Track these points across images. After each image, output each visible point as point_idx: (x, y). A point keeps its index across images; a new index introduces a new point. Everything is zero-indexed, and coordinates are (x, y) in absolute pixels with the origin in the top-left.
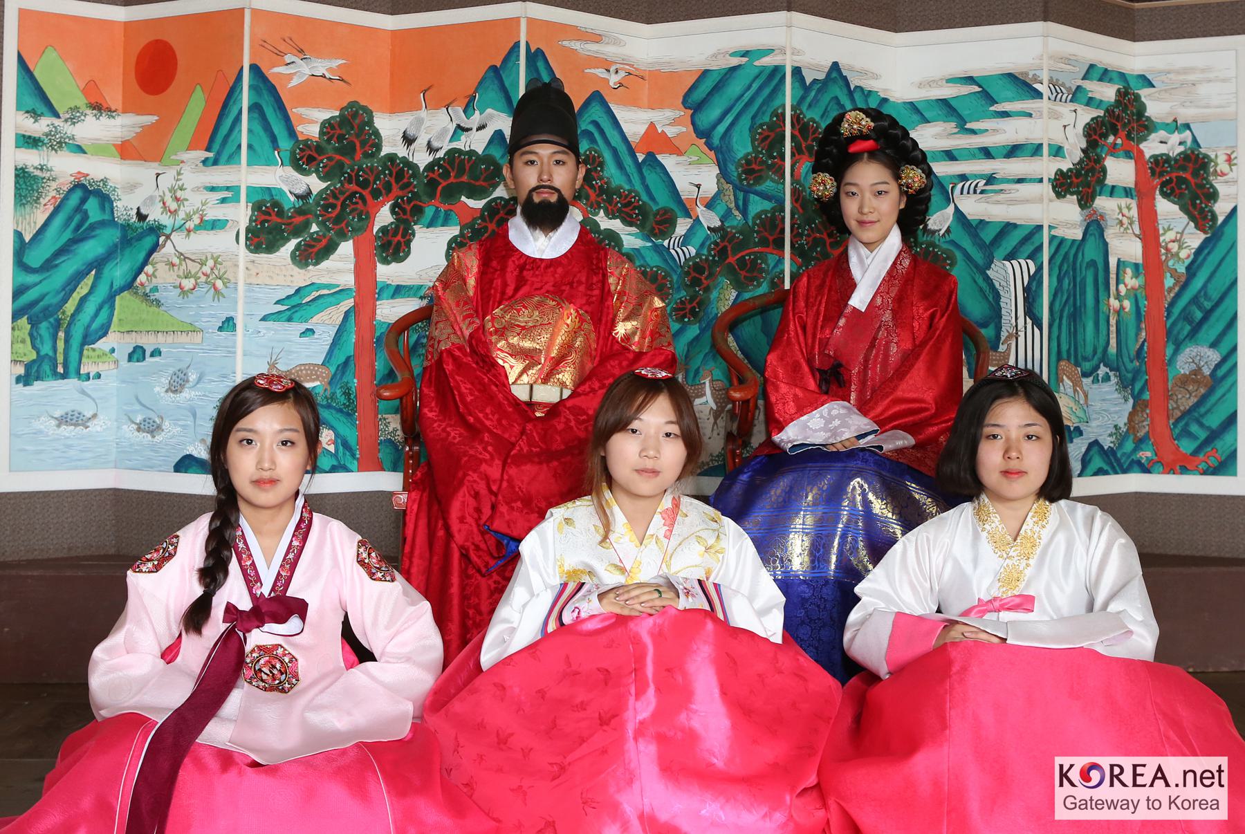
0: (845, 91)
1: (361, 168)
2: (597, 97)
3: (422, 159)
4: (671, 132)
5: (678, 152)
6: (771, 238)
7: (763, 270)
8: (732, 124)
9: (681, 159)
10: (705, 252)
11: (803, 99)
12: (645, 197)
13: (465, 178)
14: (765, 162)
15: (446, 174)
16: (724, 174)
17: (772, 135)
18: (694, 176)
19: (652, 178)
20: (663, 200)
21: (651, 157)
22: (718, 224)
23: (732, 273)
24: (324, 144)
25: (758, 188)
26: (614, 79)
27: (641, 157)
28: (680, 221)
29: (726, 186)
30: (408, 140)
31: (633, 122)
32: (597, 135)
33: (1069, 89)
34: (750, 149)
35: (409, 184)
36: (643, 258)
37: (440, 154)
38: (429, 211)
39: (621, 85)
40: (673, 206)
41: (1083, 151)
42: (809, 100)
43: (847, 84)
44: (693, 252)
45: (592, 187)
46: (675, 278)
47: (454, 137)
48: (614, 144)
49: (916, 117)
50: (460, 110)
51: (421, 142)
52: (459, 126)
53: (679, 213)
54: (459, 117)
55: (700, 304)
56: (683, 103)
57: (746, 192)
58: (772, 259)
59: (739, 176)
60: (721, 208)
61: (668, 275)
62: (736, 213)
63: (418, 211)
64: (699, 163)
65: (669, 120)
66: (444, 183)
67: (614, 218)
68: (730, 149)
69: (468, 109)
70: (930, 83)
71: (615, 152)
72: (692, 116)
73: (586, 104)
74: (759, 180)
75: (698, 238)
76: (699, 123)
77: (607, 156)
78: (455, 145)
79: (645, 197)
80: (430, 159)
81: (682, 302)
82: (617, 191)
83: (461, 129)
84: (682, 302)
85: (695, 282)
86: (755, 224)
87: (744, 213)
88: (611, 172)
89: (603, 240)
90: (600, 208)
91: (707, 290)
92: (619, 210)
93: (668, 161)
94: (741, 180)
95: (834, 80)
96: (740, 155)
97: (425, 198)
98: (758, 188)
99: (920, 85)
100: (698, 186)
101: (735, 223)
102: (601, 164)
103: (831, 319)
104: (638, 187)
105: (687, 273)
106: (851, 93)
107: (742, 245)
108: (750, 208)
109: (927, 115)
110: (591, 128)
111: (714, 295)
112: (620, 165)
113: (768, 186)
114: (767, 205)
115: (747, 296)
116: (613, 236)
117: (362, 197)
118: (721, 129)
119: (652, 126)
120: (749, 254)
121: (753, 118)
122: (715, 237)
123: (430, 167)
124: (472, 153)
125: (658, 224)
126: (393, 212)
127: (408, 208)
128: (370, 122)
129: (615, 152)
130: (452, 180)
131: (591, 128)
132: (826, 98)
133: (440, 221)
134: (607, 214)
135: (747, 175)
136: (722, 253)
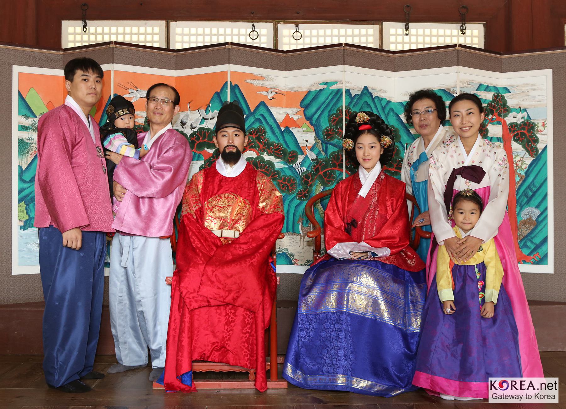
2: (262, 104)
3: (189, 132)
4: (295, 118)
5: (299, 127)
6: (337, 164)
7: (334, 178)
8: (321, 114)
9: (299, 129)
10: (310, 169)
11: (350, 103)
12: (285, 146)
14: (334, 131)
15: (198, 138)
16: (317, 136)
17: (337, 119)
18: (305, 137)
19: (288, 138)
20: (292, 147)
21: (287, 129)
24: (147, 126)
25: (332, 142)
26: (270, 96)
27: (283, 129)
28: (299, 156)
29: (318, 141)
31: (279, 113)
32: (263, 120)
34: (328, 125)
36: (284, 172)
37: (196, 130)
39: (273, 98)
42: (353, 103)
44: (305, 170)
45: (261, 142)
46: (298, 181)
47: (201, 122)
50: (204, 111)
52: (203, 118)
53: (299, 153)
54: (203, 114)
55: (308, 192)
56: (301, 105)
57: (327, 144)
58: (338, 173)
59: (324, 136)
60: (316, 151)
61: (295, 179)
62: (323, 153)
64: (307, 131)
65: (295, 113)
66: (198, 142)
67: (271, 155)
68: (320, 125)
69: (207, 110)
71: (271, 127)
73: (258, 107)
74: (332, 138)
76: (307, 114)
77: (268, 129)
78: (202, 126)
79: (285, 146)
80: (192, 132)
82: (272, 144)
83: (204, 119)
85: (306, 183)
86: (330, 157)
87: (326, 152)
88: (270, 136)
89: (266, 165)
90: (264, 151)
91: (311, 186)
92: (273, 152)
93: (294, 130)
94: (325, 139)
95: (365, 94)
96: (324, 128)
98: (332, 142)
100: (307, 141)
101: (322, 157)
102: (265, 133)
104: (282, 141)
105: (303, 179)
106: (373, 99)
107: (325, 166)
108: (328, 150)
110: (260, 117)
111: (314, 188)
112: (273, 133)
113: (335, 141)
114: (336, 149)
115: (327, 188)
116: (270, 163)
118: (316, 116)
120: (328, 171)
121: (329, 111)
123: (192, 135)
124: (209, 129)
125: (290, 157)
129: (271, 127)
130: (201, 141)
131: (260, 117)
132: (361, 102)
133: (196, 158)
134: (268, 154)
136: (317, 170)
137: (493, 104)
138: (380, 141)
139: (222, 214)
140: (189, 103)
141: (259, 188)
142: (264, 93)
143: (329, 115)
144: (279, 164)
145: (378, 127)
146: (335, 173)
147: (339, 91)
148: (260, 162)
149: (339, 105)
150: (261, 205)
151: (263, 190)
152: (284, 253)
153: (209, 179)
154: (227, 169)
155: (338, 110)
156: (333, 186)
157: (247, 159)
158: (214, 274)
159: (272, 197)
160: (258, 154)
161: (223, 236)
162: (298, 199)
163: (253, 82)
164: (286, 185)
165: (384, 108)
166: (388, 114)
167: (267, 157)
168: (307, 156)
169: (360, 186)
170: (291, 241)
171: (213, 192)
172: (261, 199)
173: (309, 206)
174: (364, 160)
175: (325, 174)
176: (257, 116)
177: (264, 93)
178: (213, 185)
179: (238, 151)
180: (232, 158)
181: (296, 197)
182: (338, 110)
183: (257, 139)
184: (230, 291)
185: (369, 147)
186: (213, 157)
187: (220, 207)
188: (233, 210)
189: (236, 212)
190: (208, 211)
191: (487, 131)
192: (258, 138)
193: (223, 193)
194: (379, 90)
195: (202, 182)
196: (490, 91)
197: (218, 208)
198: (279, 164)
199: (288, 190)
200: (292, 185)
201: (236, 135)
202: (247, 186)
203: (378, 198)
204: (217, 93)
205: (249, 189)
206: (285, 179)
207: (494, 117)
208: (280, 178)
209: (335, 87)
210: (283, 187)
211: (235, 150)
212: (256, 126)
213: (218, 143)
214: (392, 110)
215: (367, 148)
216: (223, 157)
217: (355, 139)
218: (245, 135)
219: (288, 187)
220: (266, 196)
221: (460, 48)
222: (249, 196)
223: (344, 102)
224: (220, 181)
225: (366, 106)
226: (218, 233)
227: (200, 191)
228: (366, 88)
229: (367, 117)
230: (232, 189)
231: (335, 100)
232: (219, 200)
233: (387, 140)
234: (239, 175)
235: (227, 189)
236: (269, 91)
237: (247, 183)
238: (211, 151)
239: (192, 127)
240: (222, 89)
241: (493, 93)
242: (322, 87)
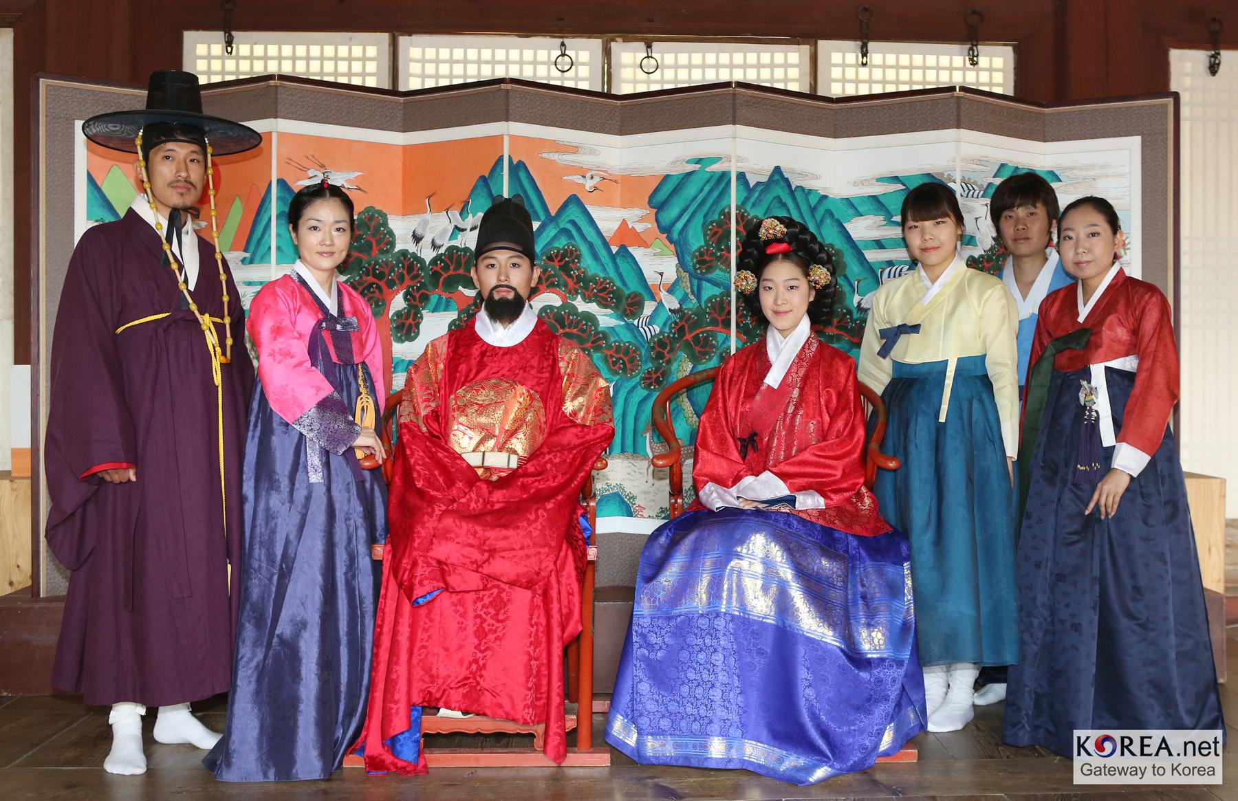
0: (787, 191)
1: (377, 263)
2: (574, 200)
3: (428, 255)
4: (639, 227)
5: (645, 245)
7: (713, 346)
8: (688, 221)
10: (667, 330)
11: (746, 199)
12: (618, 283)
13: (461, 271)
14: (714, 254)
15: (446, 268)
16: (682, 264)
18: (658, 265)
19: (624, 267)
20: (633, 286)
21: (623, 249)
22: (677, 306)
23: (688, 347)
25: (710, 276)
26: (589, 184)
27: (614, 249)
28: (647, 304)
29: (684, 274)
30: (417, 238)
31: (608, 219)
32: (574, 233)
33: (980, 187)
34: (703, 243)
35: (417, 276)
37: (442, 251)
38: (434, 298)
39: (596, 188)
40: (640, 290)
41: (994, 239)
43: (789, 185)
45: (570, 276)
46: (643, 352)
47: (452, 237)
48: (589, 239)
49: (851, 211)
50: (457, 213)
51: (427, 241)
52: (456, 227)
53: (646, 297)
55: (663, 374)
56: (650, 202)
57: (700, 279)
58: (721, 336)
60: (680, 293)
61: (637, 349)
62: (692, 297)
63: (425, 298)
64: (661, 254)
65: (638, 218)
66: (445, 275)
67: (591, 301)
68: (686, 243)
70: (863, 182)
74: (710, 269)
76: (661, 220)
77: (584, 249)
78: (453, 243)
79: (618, 283)
80: (434, 254)
82: (593, 279)
85: (660, 356)
87: (698, 296)
88: (588, 264)
90: (577, 293)
91: (669, 362)
93: (637, 252)
95: (776, 182)
96: (695, 247)
97: (430, 288)
98: (710, 276)
99: (855, 184)
101: (691, 306)
102: (579, 257)
103: (750, 396)
104: (612, 274)
105: (653, 348)
107: (697, 324)
109: (860, 209)
110: (569, 227)
111: (674, 366)
112: (596, 257)
113: (717, 274)
114: (717, 291)
115: (700, 368)
116: (589, 317)
117: (379, 287)
118: (679, 225)
119: (624, 222)
121: (705, 216)
122: (675, 318)
123: (434, 261)
124: (467, 249)
125: (629, 306)
126: (405, 299)
127: (417, 296)
128: (385, 224)
130: (451, 272)
131: (569, 227)
132: (769, 198)
133: (443, 306)
134: (584, 299)
135: (701, 265)
136: (681, 331)
138: (807, 275)
139: (483, 420)
140: (429, 197)
141: (563, 371)
142: (577, 179)
143: (704, 224)
144: (606, 319)
145: (804, 248)
146: (715, 338)
147: (724, 177)
148: (569, 314)
149: (724, 204)
153: (461, 351)
154: (495, 330)
155: (722, 213)
156: (713, 363)
157: (544, 309)
160: (564, 299)
161: (486, 464)
162: (645, 388)
163: (554, 157)
164: (622, 359)
165: (813, 210)
166: (822, 221)
167: (581, 305)
168: (661, 303)
169: (767, 366)
170: (629, 470)
171: (467, 376)
173: (661, 404)
174: (777, 313)
175: (696, 338)
176: (563, 224)
177: (577, 179)
181: (639, 383)
182: (722, 213)
183: (562, 269)
185: (787, 289)
186: (475, 304)
187: (481, 405)
188: (506, 412)
189: (512, 416)
190: (456, 414)
192: (566, 268)
193: (487, 378)
194: (804, 175)
197: (476, 407)
198: (606, 319)
199: (624, 370)
200: (632, 360)
202: (535, 364)
203: (802, 389)
204: (483, 178)
205: (541, 371)
206: (618, 348)
208: (609, 347)
209: (717, 168)
210: (614, 363)
212: (562, 243)
213: (479, 280)
214: (829, 213)
215: (782, 289)
216: (487, 308)
217: (758, 271)
218: (533, 265)
219: (624, 363)
221: (962, 94)
222: (539, 384)
223: (734, 197)
224: (483, 354)
225: (778, 205)
226: (473, 460)
228: (777, 170)
229: (780, 228)
231: (716, 194)
233: (821, 274)
234: (521, 344)
235: (494, 370)
236: (588, 175)
237: (536, 359)
238: (471, 293)
242: (690, 168)
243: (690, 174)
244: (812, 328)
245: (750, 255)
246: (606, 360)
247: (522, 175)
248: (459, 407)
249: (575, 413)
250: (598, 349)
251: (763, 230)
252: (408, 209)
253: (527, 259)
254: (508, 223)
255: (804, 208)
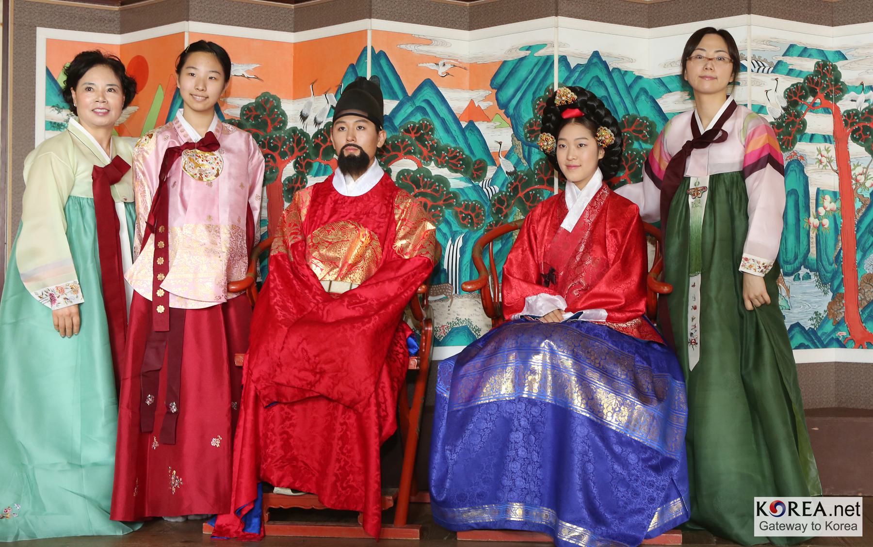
0: (605, 71)
1: (271, 138)
2: (428, 83)
5: (488, 120)
8: (521, 98)
16: (516, 134)
18: (498, 136)
22: (512, 169)
26: (442, 70)
29: (518, 142)
30: (304, 117)
32: (428, 110)
33: (770, 64)
35: (304, 148)
37: (322, 126)
38: (316, 165)
39: (448, 74)
41: (784, 109)
43: (607, 67)
44: (497, 190)
45: (425, 146)
46: (486, 208)
48: (442, 115)
51: (311, 119)
53: (488, 163)
60: (514, 158)
61: (482, 206)
63: (309, 165)
64: (500, 127)
66: (324, 146)
67: (443, 167)
68: (519, 117)
72: (496, 93)
73: (420, 88)
75: (500, 181)
76: (500, 98)
77: (437, 124)
80: (316, 130)
81: (491, 225)
82: (446, 148)
84: (491, 225)
85: (499, 211)
88: (440, 136)
89: (434, 183)
90: (431, 160)
92: (446, 162)
95: (595, 64)
97: (313, 157)
105: (494, 205)
106: (609, 73)
110: (424, 105)
112: (447, 130)
116: (442, 180)
117: (273, 157)
118: (514, 102)
123: (316, 135)
126: (295, 167)
127: (303, 163)
128: (278, 106)
131: (424, 105)
133: (322, 172)
136: (515, 189)
137: (816, 78)
138: (595, 136)
140: (313, 84)
141: (397, 217)
142: (431, 66)
143: (533, 100)
144: (456, 181)
145: (592, 111)
146: (542, 195)
147: (548, 59)
148: (424, 176)
149: (548, 82)
150: (399, 244)
151: (404, 220)
152: (465, 328)
153: (319, 200)
155: (547, 90)
158: (301, 346)
159: (418, 231)
160: (419, 164)
164: (469, 215)
165: (629, 88)
166: (637, 97)
167: (435, 170)
168: (500, 167)
169: (563, 212)
172: (401, 234)
174: (568, 167)
175: (527, 195)
177: (431, 66)
178: (323, 208)
179: (363, 154)
180: (354, 165)
182: (547, 90)
184: (322, 373)
185: (579, 147)
187: (330, 243)
188: (350, 250)
189: (355, 252)
190: (311, 249)
191: (804, 124)
193: (337, 221)
194: (621, 58)
195: (308, 203)
196: (810, 56)
197: (327, 244)
198: (456, 181)
199: (472, 224)
200: (478, 216)
201: (360, 127)
204: (352, 66)
206: (467, 207)
207: (818, 101)
208: (459, 204)
209: (543, 53)
210: (464, 219)
211: (357, 153)
212: (417, 118)
214: (644, 91)
215: (573, 147)
217: (556, 134)
218: (378, 130)
220: (408, 229)
223: (557, 76)
225: (597, 83)
227: (303, 219)
228: (596, 54)
229: (572, 96)
230: (352, 215)
231: (542, 74)
232: (329, 231)
233: (607, 135)
234: (366, 194)
236: (441, 63)
239: (317, 123)
240: (359, 60)
241: (815, 61)
242: (523, 54)
243: (522, 59)
244: (604, 180)
245: (549, 120)
246: (456, 215)
247: (383, 62)
248: (314, 245)
249: (402, 249)
250: (449, 206)
251: (557, 98)
252: (298, 94)
253: (373, 124)
254: (360, 98)
255: (621, 87)
